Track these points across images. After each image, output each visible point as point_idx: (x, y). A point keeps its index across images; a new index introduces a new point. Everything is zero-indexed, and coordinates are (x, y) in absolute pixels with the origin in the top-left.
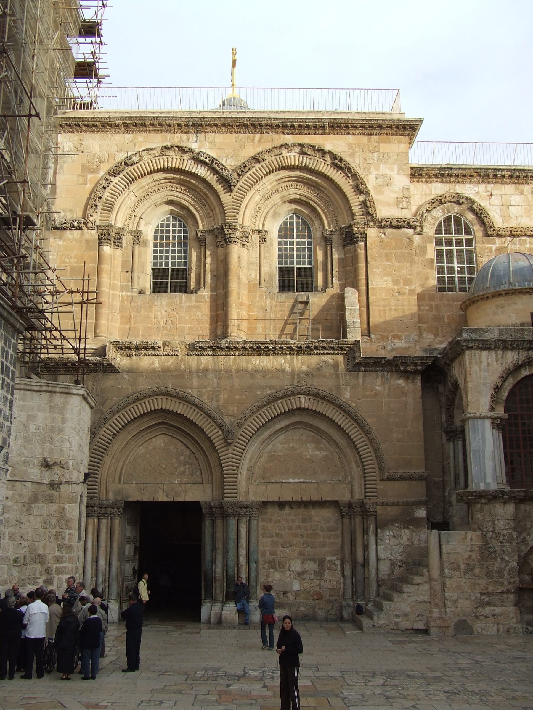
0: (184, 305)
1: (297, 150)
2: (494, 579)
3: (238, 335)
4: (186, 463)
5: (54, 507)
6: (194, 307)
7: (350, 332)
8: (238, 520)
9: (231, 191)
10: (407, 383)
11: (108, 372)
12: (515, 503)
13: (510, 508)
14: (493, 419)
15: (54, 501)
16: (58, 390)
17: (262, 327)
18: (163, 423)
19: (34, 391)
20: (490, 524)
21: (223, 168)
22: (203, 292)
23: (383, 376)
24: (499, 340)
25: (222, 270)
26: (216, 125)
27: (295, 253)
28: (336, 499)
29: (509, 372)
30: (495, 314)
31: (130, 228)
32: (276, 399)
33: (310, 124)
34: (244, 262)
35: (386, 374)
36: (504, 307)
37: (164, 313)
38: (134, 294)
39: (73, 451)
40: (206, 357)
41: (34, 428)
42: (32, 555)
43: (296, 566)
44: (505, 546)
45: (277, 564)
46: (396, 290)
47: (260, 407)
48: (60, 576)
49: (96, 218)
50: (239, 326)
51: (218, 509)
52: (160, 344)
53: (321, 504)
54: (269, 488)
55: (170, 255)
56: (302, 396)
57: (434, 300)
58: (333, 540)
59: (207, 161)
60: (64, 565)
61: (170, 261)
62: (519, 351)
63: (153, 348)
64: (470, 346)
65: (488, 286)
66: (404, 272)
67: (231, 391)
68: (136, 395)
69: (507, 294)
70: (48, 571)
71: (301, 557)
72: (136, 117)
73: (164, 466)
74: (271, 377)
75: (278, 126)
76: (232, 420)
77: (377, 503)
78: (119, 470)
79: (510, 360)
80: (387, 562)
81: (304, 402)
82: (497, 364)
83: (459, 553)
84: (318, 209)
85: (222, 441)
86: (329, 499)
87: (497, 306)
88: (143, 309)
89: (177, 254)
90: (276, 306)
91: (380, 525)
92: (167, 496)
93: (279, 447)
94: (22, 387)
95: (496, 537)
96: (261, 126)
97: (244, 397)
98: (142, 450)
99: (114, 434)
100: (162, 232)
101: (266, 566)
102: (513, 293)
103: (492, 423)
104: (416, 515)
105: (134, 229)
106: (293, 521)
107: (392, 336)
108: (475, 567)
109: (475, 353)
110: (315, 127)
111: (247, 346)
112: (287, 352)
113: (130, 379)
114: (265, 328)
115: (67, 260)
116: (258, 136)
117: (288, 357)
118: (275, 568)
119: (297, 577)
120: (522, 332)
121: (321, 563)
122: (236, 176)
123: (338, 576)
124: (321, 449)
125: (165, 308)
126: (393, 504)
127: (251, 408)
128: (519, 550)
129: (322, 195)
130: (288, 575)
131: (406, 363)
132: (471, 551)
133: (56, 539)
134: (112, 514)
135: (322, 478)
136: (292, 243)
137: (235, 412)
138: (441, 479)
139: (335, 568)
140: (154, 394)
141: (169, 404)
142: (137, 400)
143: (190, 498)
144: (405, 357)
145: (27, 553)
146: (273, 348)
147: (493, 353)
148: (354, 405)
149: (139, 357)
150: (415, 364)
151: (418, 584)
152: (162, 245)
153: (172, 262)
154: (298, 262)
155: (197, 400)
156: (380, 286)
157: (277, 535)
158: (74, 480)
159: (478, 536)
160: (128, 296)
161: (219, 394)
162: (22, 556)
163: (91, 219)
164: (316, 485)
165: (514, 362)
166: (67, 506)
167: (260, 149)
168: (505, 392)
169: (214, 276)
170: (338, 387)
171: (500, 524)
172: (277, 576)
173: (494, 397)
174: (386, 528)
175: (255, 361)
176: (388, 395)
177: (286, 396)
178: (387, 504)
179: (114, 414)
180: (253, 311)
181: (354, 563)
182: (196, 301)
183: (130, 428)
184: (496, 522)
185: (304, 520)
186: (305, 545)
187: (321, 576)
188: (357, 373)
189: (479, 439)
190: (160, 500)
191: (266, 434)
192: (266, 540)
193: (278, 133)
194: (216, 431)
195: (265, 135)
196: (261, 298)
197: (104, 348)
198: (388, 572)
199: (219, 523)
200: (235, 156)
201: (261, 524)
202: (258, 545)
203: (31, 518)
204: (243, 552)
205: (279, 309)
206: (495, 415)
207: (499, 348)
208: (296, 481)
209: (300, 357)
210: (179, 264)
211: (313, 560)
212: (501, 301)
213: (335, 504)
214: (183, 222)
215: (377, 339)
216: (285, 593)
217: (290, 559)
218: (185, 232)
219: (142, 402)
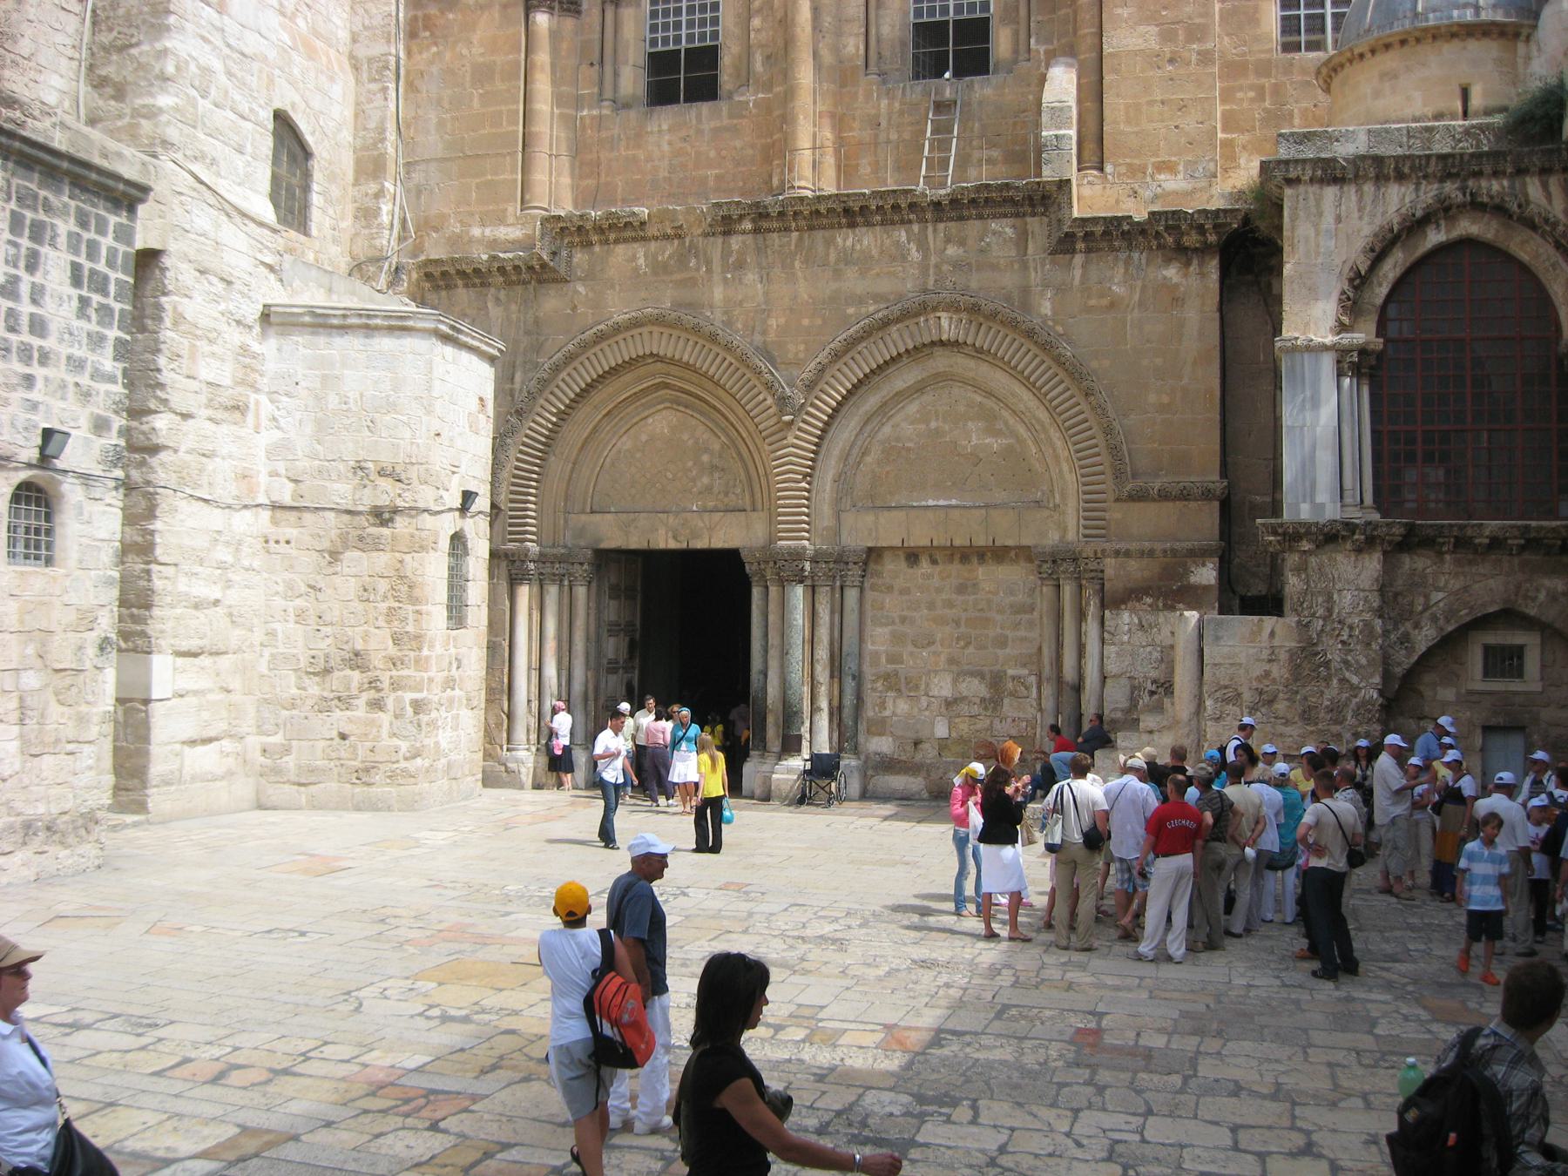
2: (1320, 726)
3: (814, 184)
4: (714, 468)
5: (382, 560)
7: (1048, 162)
8: (813, 587)
10: (1186, 276)
11: (545, 281)
12: (1385, 553)
13: (1372, 564)
14: (1341, 352)
15: (382, 547)
16: (379, 321)
17: (870, 164)
18: (667, 386)
19: (332, 327)
20: (1320, 600)
22: (742, 95)
23: (1127, 262)
24: (1363, 158)
25: (780, 43)
28: (1026, 542)
29: (1389, 236)
30: (1377, 94)
32: (886, 323)
34: (829, 19)
35: (1136, 255)
36: (1396, 77)
37: (666, 148)
38: (606, 112)
39: (418, 445)
40: (741, 238)
41: (337, 401)
42: (343, 653)
43: (943, 687)
44: (1351, 651)
45: (903, 680)
46: (1168, 56)
47: (852, 343)
48: (400, 693)
51: (771, 564)
52: (643, 212)
53: (999, 554)
54: (882, 520)
55: (684, 18)
56: (943, 315)
57: (1269, 75)
58: (1022, 633)
60: (405, 672)
61: (684, 32)
62: (1418, 185)
64: (1292, 175)
65: (1367, 27)
66: (1187, 9)
67: (791, 310)
68: (600, 327)
69: (1403, 42)
70: (373, 684)
71: (954, 668)
73: (670, 475)
74: (878, 275)
77: (1103, 551)
79: (1392, 209)
80: (1124, 681)
81: (947, 325)
82: (1360, 218)
83: (1240, 665)
85: (773, 420)
86: (1010, 542)
87: (1384, 76)
88: (623, 143)
89: (697, 16)
90: (901, 113)
91: (1111, 601)
92: (675, 538)
93: (908, 429)
94: (307, 319)
95: (1334, 629)
97: (819, 322)
98: (626, 443)
101: (879, 685)
102: (1418, 40)
103: (1338, 362)
104: (1193, 579)
106: (939, 590)
107: (1153, 164)
108: (1276, 697)
109: (1306, 192)
111: (823, 209)
112: (912, 216)
113: (590, 295)
114: (877, 167)
115: (465, 51)
117: (916, 228)
118: (899, 690)
119: (943, 709)
120: (1427, 135)
121: (996, 681)
123: (1031, 711)
124: (997, 434)
126: (1142, 554)
127: (832, 345)
128: (1386, 660)
130: (925, 704)
131: (1179, 227)
132: (1270, 661)
133: (389, 622)
134: (570, 575)
135: (999, 496)
137: (801, 355)
138: (1268, 499)
139: (1025, 693)
140: (635, 324)
141: (663, 343)
142: (600, 338)
143: (718, 543)
144: (1174, 212)
145: (333, 650)
147: (1351, 190)
148: (1060, 329)
149: (606, 247)
150: (1201, 229)
151: (1151, 732)
153: (687, 35)
155: (720, 332)
156: (1130, 48)
157: (903, 620)
158: (421, 505)
159: (1289, 626)
160: (593, 118)
161: (768, 316)
162: (321, 654)
164: (983, 511)
165: (1403, 210)
166: (408, 558)
168: (1380, 285)
170: (1025, 290)
171: (1345, 600)
172: (903, 706)
173: (1349, 299)
174: (1123, 607)
175: (845, 240)
176: (1141, 303)
177: (906, 315)
178: (1127, 554)
179: (556, 369)
180: (851, 129)
181: (1059, 679)
182: (731, 117)
183: (596, 397)
184: (1335, 596)
185: (961, 589)
186: (962, 643)
187: (995, 709)
188: (1068, 256)
189: (1303, 401)
190: (662, 546)
191: (871, 401)
192: (879, 630)
194: (761, 397)
196: (868, 96)
198: (1125, 704)
199: (774, 590)
201: (870, 595)
202: (861, 640)
203: (337, 580)
204: (822, 653)
206: (1345, 342)
207: (1366, 178)
208: (942, 503)
209: (941, 226)
210: (703, 37)
211: (980, 675)
212: (1389, 61)
213: (1024, 553)
215: (1119, 175)
216: (916, 744)
217: (929, 671)
219: (611, 341)
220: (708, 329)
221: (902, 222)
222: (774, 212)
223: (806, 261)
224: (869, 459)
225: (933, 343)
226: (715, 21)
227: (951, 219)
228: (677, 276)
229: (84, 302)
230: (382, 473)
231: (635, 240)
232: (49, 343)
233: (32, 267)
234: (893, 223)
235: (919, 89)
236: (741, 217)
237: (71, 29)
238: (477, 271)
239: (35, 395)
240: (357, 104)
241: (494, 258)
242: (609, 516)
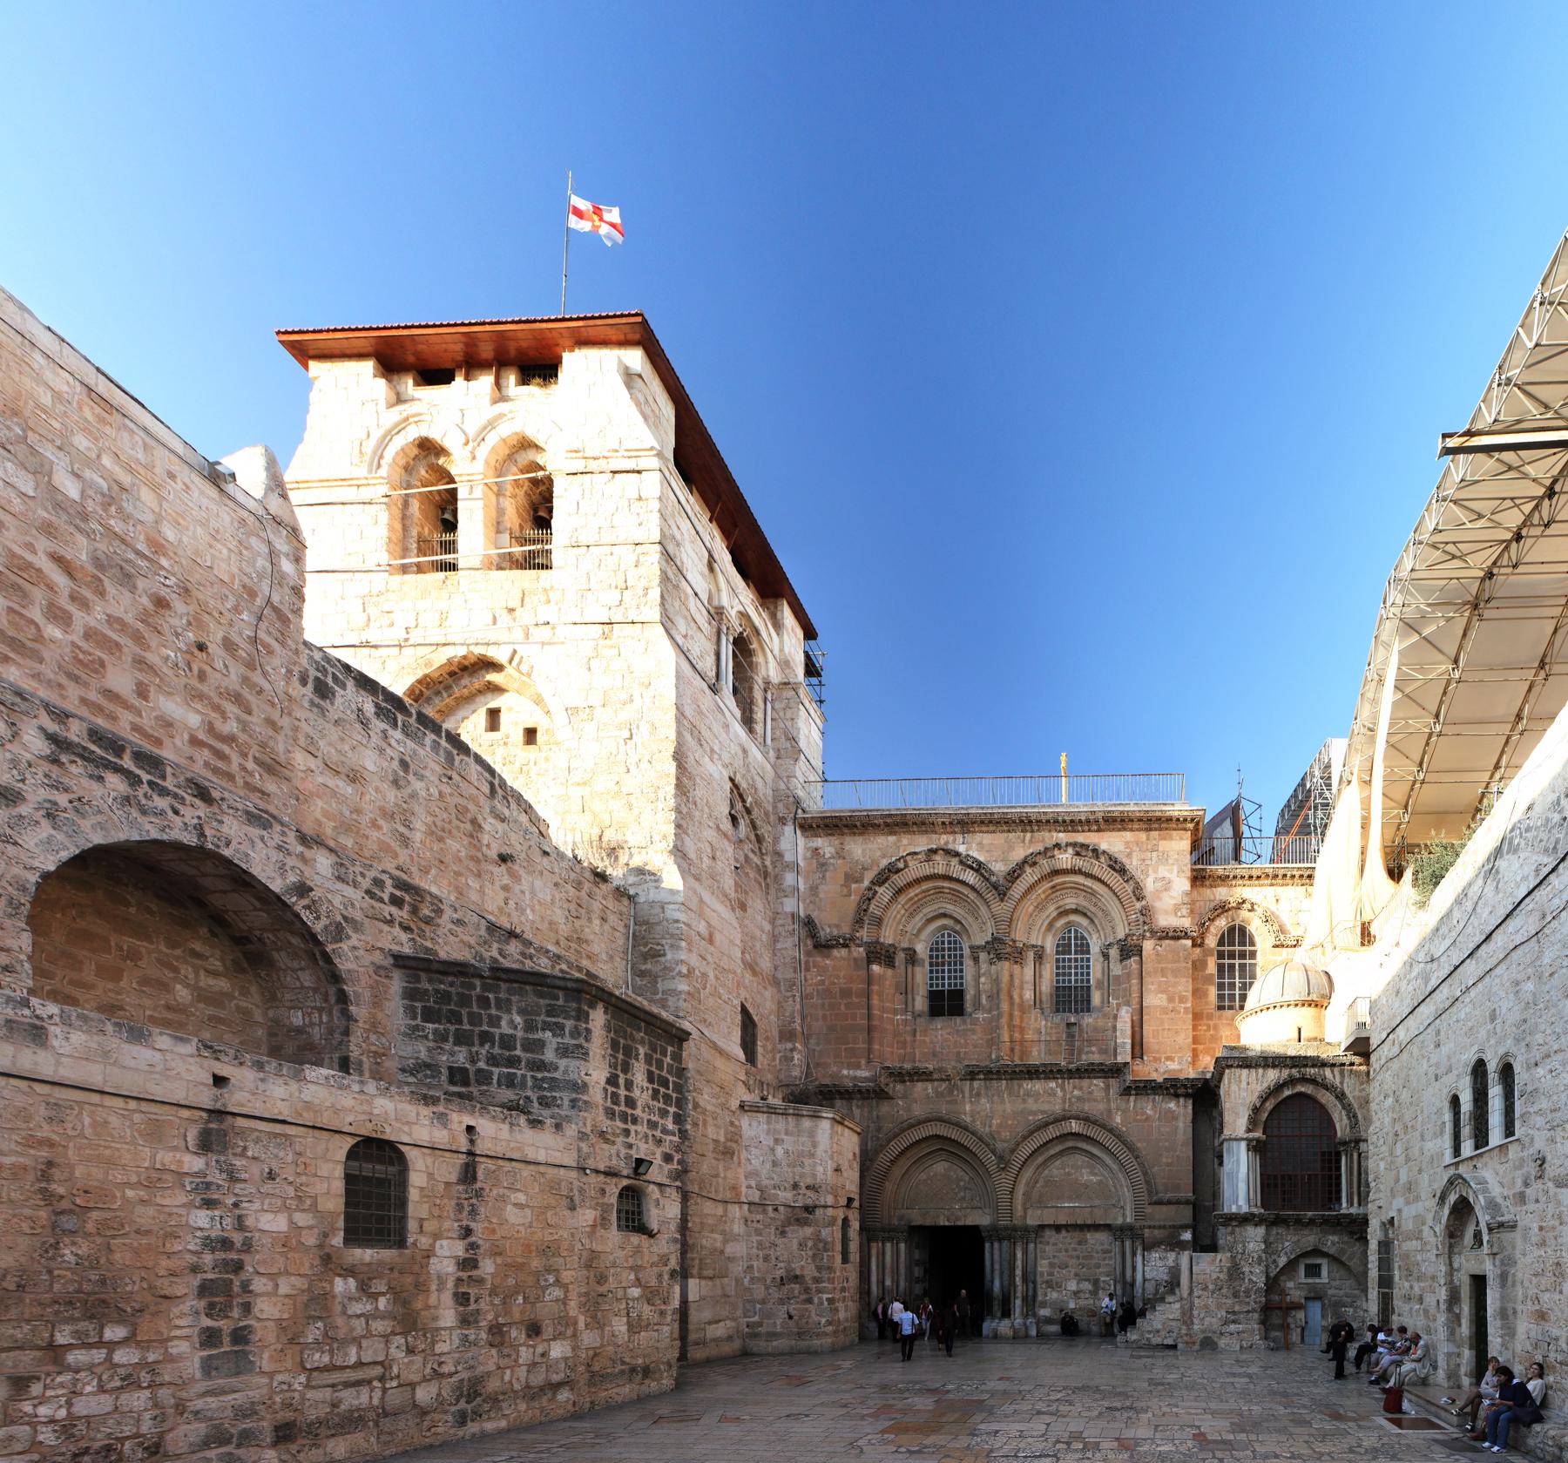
1: (1070, 850)
9: (1002, 900)
31: (903, 945)
33: (1083, 818)
49: (864, 934)
50: (1012, 1050)
100: (937, 950)
105: (905, 945)
110: (1088, 821)
122: (1006, 883)
152: (937, 965)
195: (1036, 834)
200: (1004, 860)
214: (958, 938)
218: (961, 949)
240: (779, 1003)
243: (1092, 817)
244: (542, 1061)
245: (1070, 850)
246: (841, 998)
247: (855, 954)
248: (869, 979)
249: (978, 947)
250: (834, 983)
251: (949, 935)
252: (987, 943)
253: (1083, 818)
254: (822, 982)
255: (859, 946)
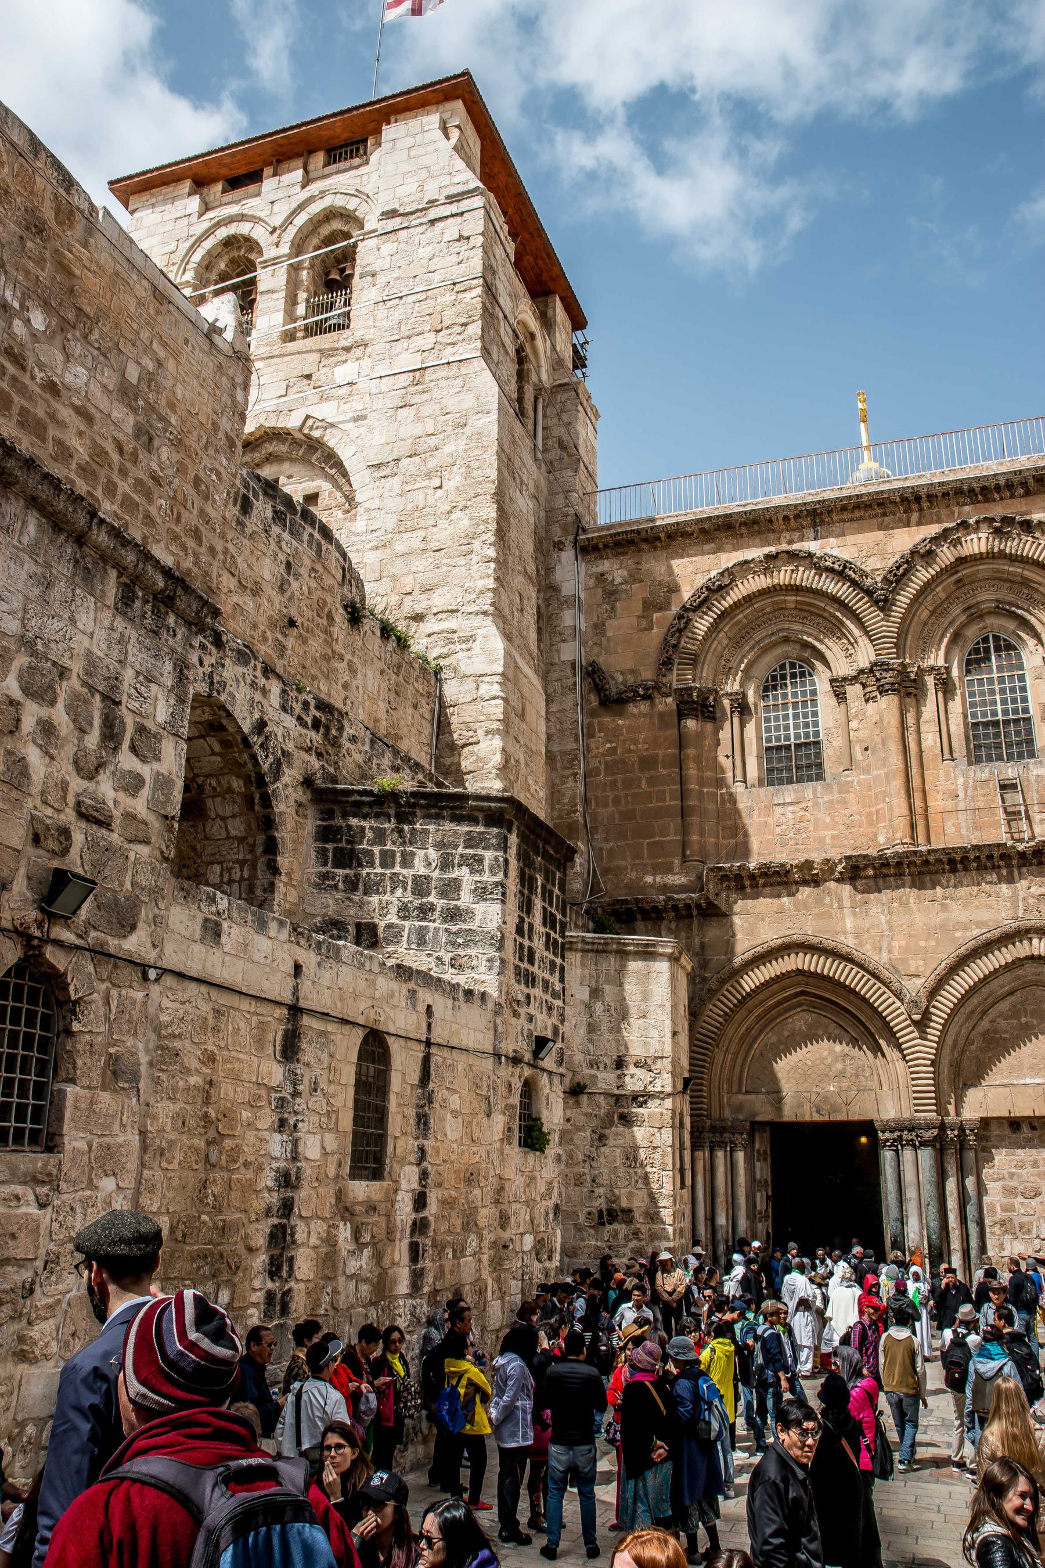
0: (821, 801)
6: (838, 802)
21: (864, 574)
26: (844, 508)
27: (998, 697)
33: (1002, 483)
37: (790, 815)
54: (990, 1095)
55: (791, 722)
59: (836, 566)
61: (792, 732)
63: (778, 872)
67: (910, 935)
72: (718, 517)
75: (945, 495)
76: (918, 982)
78: (737, 1070)
84: (1033, 620)
90: (975, 788)
92: (818, 1112)
94: (580, 946)
96: (918, 499)
97: (933, 943)
99: (726, 1013)
110: (1010, 486)
111: (931, 858)
115: (632, 747)
116: (915, 516)
125: (790, 808)
129: (1035, 596)
134: (732, 1142)
136: (991, 681)
137: (921, 969)
145: (604, 1207)
146: (977, 858)
154: (1005, 712)
157: (1012, 1175)
163: (664, 680)
167: (922, 536)
169: (866, 749)
177: (1007, 938)
180: (936, 800)
190: (808, 1119)
193: (948, 506)
194: (890, 1001)
197: (700, 877)
205: (980, 792)
208: (1037, 1081)
214: (807, 668)
220: (844, 950)
221: (994, 867)
222: (892, 862)
223: (918, 898)
224: (973, 1048)
225: (1026, 958)
226: (816, 724)
227: (1031, 865)
228: (816, 911)
229: (548, 935)
230: (636, 1065)
231: (779, 884)
232: (535, 969)
233: (529, 912)
234: (986, 868)
235: (987, 770)
236: (866, 867)
237: (427, 732)
238: (655, 909)
239: (532, 1010)
241: (670, 898)
242: (761, 1096)
243: (1016, 479)
244: (457, 908)
245: (984, 527)
246: (641, 770)
247: (660, 707)
248: (681, 742)
249: (845, 679)
250: (630, 751)
251: (793, 666)
252: (862, 672)
253: (1002, 483)
254: (613, 751)
255: (667, 695)
